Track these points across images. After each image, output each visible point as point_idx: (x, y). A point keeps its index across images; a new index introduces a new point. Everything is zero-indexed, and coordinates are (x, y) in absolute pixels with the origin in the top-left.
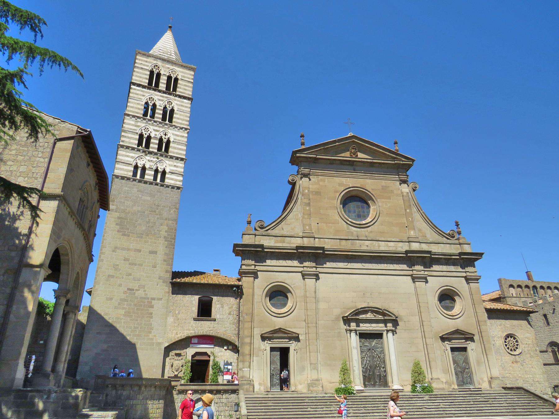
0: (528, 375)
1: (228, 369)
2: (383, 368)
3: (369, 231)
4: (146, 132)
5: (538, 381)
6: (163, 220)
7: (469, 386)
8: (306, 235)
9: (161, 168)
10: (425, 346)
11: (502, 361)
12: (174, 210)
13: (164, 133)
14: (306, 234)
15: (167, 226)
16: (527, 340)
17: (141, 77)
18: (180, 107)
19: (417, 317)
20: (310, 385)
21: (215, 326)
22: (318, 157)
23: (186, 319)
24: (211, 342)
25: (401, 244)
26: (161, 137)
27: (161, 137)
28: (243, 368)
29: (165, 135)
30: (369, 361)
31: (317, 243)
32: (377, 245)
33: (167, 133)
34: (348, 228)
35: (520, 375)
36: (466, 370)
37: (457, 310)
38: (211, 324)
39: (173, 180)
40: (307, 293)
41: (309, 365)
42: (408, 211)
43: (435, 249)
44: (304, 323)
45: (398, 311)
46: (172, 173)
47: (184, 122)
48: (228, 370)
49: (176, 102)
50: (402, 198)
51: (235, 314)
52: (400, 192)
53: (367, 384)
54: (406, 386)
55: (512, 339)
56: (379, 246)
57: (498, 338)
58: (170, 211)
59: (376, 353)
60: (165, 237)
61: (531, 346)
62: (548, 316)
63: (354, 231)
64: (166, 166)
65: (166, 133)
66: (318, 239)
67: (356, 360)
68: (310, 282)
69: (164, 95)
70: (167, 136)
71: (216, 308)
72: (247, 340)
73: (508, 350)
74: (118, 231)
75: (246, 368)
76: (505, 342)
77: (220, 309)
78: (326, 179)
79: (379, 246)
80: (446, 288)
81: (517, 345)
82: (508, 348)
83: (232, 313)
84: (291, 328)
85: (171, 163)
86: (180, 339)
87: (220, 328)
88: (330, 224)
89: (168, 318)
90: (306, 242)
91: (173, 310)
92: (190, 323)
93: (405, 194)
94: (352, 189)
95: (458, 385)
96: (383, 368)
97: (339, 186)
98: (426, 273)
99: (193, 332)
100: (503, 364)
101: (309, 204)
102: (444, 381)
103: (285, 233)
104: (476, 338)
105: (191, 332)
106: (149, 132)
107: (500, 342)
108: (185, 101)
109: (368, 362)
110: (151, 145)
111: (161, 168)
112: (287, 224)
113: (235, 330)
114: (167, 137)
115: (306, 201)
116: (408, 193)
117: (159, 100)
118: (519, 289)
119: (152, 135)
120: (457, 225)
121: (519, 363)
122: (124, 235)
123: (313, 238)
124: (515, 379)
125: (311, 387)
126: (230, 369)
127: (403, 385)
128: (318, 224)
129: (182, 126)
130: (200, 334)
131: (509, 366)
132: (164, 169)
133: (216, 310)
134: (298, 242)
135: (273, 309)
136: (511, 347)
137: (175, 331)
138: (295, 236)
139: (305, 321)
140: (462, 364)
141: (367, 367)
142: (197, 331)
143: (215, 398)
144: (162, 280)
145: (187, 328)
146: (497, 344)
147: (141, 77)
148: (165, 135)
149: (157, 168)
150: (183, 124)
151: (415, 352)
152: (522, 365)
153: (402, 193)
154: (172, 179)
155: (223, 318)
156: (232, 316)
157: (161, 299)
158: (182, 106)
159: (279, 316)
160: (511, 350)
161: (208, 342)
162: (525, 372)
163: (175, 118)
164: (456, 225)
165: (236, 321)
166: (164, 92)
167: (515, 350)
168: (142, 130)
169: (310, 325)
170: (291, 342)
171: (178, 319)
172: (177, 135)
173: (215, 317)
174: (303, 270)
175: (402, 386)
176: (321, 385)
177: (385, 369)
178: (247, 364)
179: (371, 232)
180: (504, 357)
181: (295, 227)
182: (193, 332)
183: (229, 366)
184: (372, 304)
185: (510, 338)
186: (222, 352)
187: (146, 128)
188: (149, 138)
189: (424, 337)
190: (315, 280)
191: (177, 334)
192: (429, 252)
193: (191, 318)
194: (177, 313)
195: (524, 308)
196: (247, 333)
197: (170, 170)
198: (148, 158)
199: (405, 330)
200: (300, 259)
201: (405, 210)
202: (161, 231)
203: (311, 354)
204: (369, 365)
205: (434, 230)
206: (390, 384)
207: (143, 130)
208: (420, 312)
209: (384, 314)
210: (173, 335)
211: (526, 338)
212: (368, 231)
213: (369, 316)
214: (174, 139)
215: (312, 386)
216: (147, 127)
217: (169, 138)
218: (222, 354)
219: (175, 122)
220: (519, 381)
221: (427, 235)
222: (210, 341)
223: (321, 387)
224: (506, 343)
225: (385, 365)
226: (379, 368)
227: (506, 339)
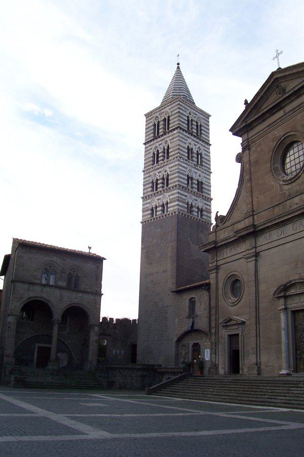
17: (149, 135)
18: (172, 141)
22: (248, 123)
34: (281, 190)
46: (171, 202)
49: (170, 138)
63: (287, 190)
69: (163, 138)
74: (147, 262)
88: (266, 193)
97: (273, 142)
108: (175, 132)
117: (160, 145)
122: (149, 264)
147: (149, 135)
154: (171, 207)
158: (173, 139)
166: (162, 136)
172: (172, 167)
181: (243, 210)
198: (157, 198)
214: (171, 171)
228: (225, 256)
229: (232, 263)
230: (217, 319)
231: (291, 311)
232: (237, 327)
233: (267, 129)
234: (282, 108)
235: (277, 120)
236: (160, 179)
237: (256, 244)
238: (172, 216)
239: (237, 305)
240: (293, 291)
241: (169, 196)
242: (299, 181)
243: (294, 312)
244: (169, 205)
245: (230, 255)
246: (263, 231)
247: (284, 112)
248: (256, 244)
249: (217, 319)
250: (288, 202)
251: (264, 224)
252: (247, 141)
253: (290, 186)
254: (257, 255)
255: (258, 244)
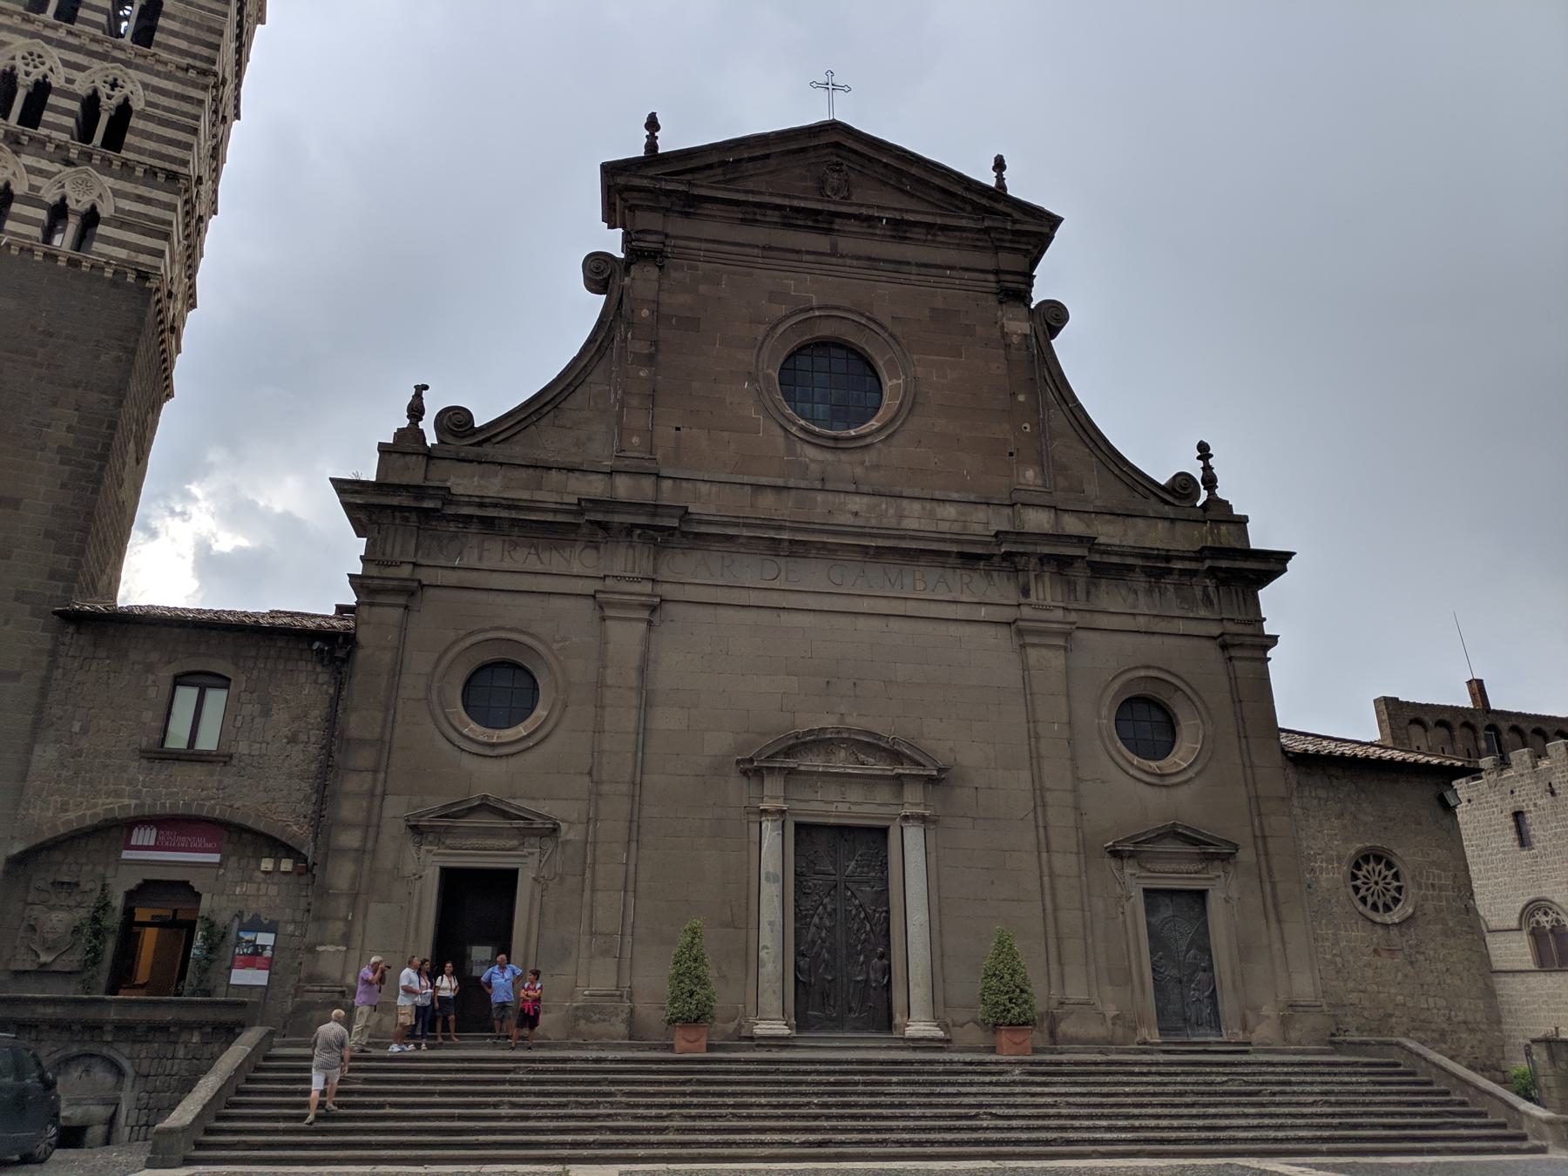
0: (1431, 1000)
1: (256, 947)
2: (882, 957)
3: (867, 464)
4: (30, 69)
5: (1465, 1023)
6: (60, 385)
7: (1207, 1035)
8: (626, 466)
9: (78, 201)
10: (1046, 879)
11: (1336, 943)
12: (114, 354)
13: (110, 79)
14: (627, 462)
15: (76, 410)
16: (1436, 872)
19: (1025, 775)
20: (580, 1013)
21: (226, 781)
22: (696, 191)
23: (108, 755)
24: (210, 845)
25: (981, 514)
26: (95, 91)
27: (95, 91)
28: (322, 944)
29: (114, 85)
30: (830, 930)
31: (668, 493)
32: (891, 511)
33: (120, 82)
35: (1400, 999)
36: (1200, 975)
37: (1181, 756)
38: (211, 774)
39: (124, 247)
40: (609, 671)
41: (585, 939)
42: (1021, 398)
43: (1109, 533)
44: (587, 779)
45: (951, 750)
46: (122, 225)
47: (197, 49)
48: (257, 950)
50: (1002, 352)
51: (313, 739)
52: (996, 333)
53: (816, 1017)
54: (962, 1026)
55: (1382, 866)
56: (901, 517)
57: (1329, 860)
58: (98, 357)
59: (857, 902)
60: (61, 449)
61: (1451, 893)
62: (1530, 818)
63: (812, 461)
64: (100, 196)
65: (116, 80)
66: (670, 482)
67: (771, 923)
68: (626, 635)
70: (117, 89)
71: (239, 718)
72: (350, 839)
73: (1361, 908)
75: (332, 943)
76: (1354, 877)
77: (257, 720)
78: (725, 276)
79: (901, 517)
80: (1142, 673)
81: (1399, 889)
82: (1364, 900)
83: (303, 737)
84: (533, 799)
85: (127, 187)
86: (75, 826)
87: (245, 790)
88: (726, 434)
89: (38, 749)
90: (624, 488)
91: (60, 718)
92: (123, 769)
93: (1015, 339)
94: (817, 313)
95: (1163, 1031)
96: (882, 957)
98: (1073, 617)
99: (133, 802)
100: (1340, 955)
101: (650, 360)
102: (1111, 1011)
103: (549, 455)
104: (1246, 855)
105: (126, 801)
106: (44, 69)
107: (1332, 878)
109: (823, 934)
110: (47, 116)
111: (78, 201)
112: (562, 427)
113: (307, 799)
114: (117, 93)
115: (641, 347)
116: (1026, 335)
118: (1443, 732)
119: (56, 81)
120: (1204, 451)
121: (1400, 955)
123: (653, 478)
124: (1381, 1012)
125: (582, 1022)
126: (264, 947)
127: (949, 1021)
128: (678, 429)
129: (190, 61)
130: (158, 810)
131: (1361, 964)
132: (94, 207)
133: (238, 724)
134: (595, 487)
135: (474, 729)
136: (1375, 897)
137: (59, 799)
138: (585, 467)
139: (590, 774)
140: (1187, 952)
141: (819, 954)
142: (149, 801)
143: (143, 1055)
144: (28, 607)
145: (112, 787)
146: (1324, 884)
148: (114, 85)
149: (63, 199)
150: (194, 56)
151: (1004, 900)
152: (1411, 963)
153: (1004, 335)
155: (261, 756)
156: (301, 746)
157: (16, 676)
159: (490, 751)
160: (1375, 907)
161: (201, 841)
162: (1422, 985)
163: (163, 30)
164: (1199, 458)
165: (313, 767)
167: (1387, 908)
168: (13, 58)
169: (605, 788)
170: (525, 851)
171: (79, 753)
173: (233, 750)
174: (602, 589)
175: (944, 1026)
176: (624, 1016)
177: (889, 960)
178: (338, 927)
179: (876, 467)
180: (1346, 930)
182: (133, 802)
183: (260, 935)
184: (853, 721)
185: (1372, 864)
186: (250, 880)
187: (31, 54)
188: (41, 90)
189: (1044, 849)
190: (644, 626)
191: (67, 811)
192: (1089, 541)
193: (133, 751)
194: (76, 727)
195: (1430, 759)
196: (348, 810)
197: (117, 209)
198: (28, 160)
199: (975, 819)
200: (597, 548)
201: (1013, 395)
202: (49, 426)
203: (599, 895)
204: (827, 944)
205: (1117, 471)
206: (898, 1019)
207: (18, 58)
208: (1036, 758)
209: (896, 756)
210: (50, 814)
211: (1433, 863)
212: (863, 463)
213: (841, 762)
214: (149, 104)
215: (588, 1020)
216: (37, 50)
217: (127, 100)
218: (251, 888)
219: (159, 45)
220: (1394, 1020)
221: (1086, 487)
222: (209, 841)
223: (623, 1021)
224: (1358, 883)
225: (888, 946)
226: (865, 956)
227: (1358, 866)
228: (471, 559)
229: (502, 598)
230: (379, 790)
231: (798, 826)
232: (515, 843)
233: (756, 251)
234: (828, 231)
235: (808, 252)
236: (71, 96)
237: (655, 571)
238: (114, 283)
239: (512, 761)
240: (811, 762)
241: (116, 193)
242: (869, 457)
243: (799, 826)
244: (101, 229)
245: (506, 565)
246: (701, 540)
247: (834, 246)
248: (655, 571)
249: (379, 790)
250: (820, 497)
251: (725, 524)
252: (661, 238)
253: (828, 456)
254: (653, 609)
255: (664, 574)
